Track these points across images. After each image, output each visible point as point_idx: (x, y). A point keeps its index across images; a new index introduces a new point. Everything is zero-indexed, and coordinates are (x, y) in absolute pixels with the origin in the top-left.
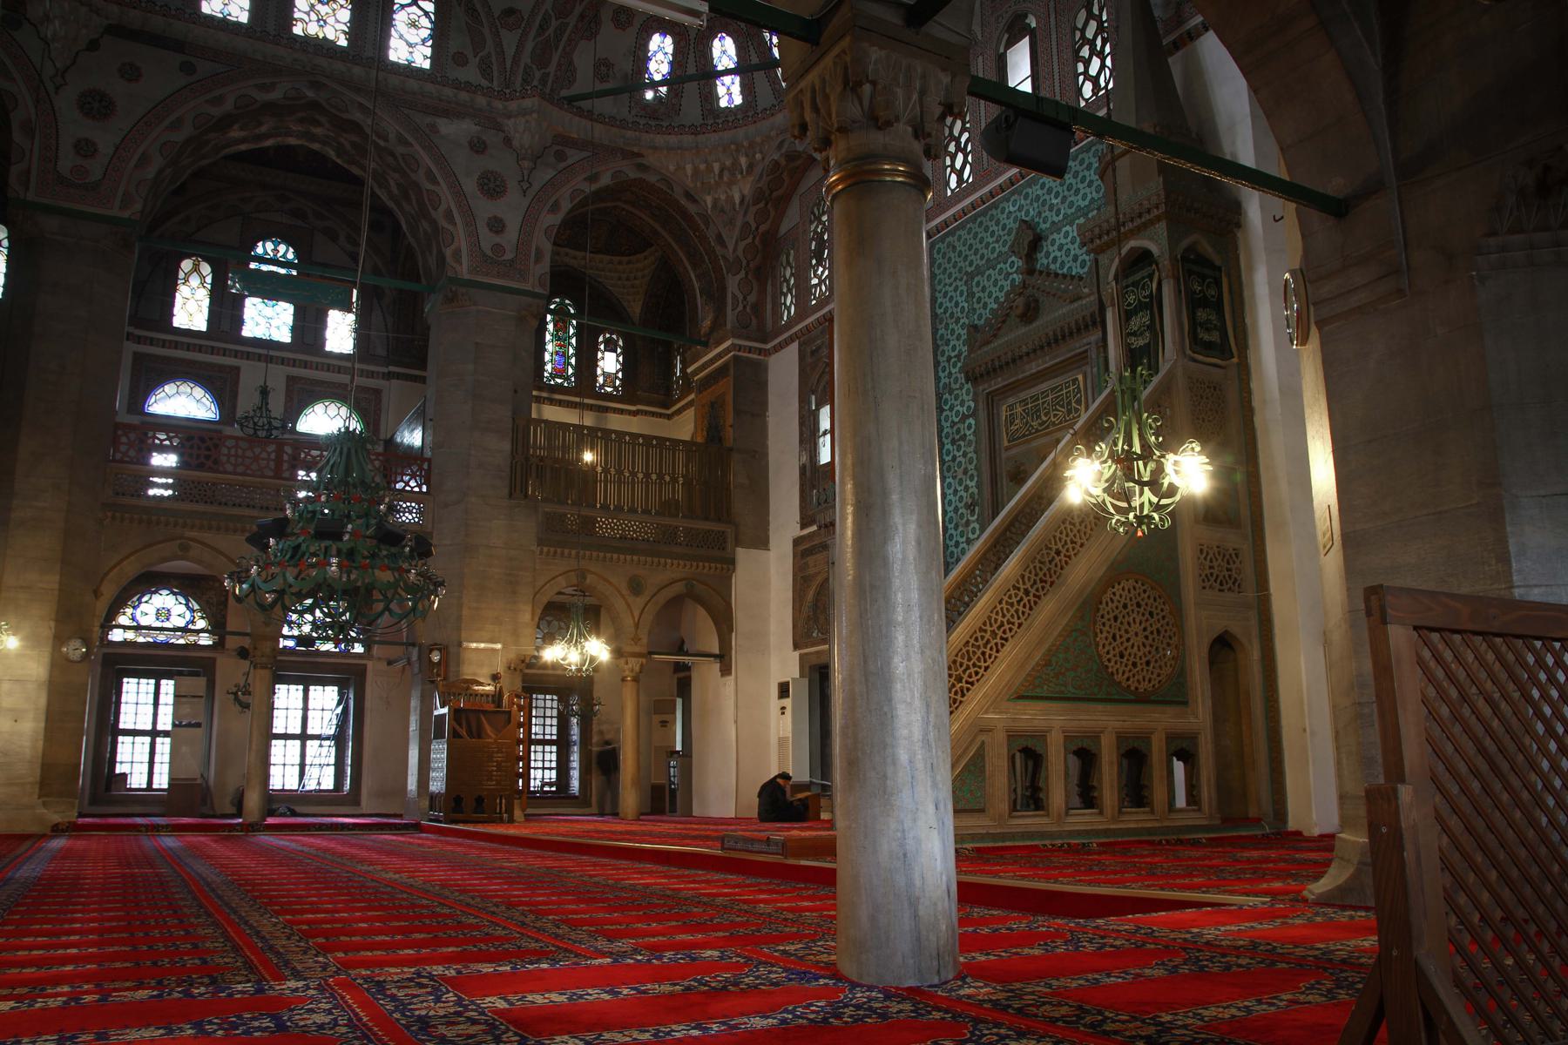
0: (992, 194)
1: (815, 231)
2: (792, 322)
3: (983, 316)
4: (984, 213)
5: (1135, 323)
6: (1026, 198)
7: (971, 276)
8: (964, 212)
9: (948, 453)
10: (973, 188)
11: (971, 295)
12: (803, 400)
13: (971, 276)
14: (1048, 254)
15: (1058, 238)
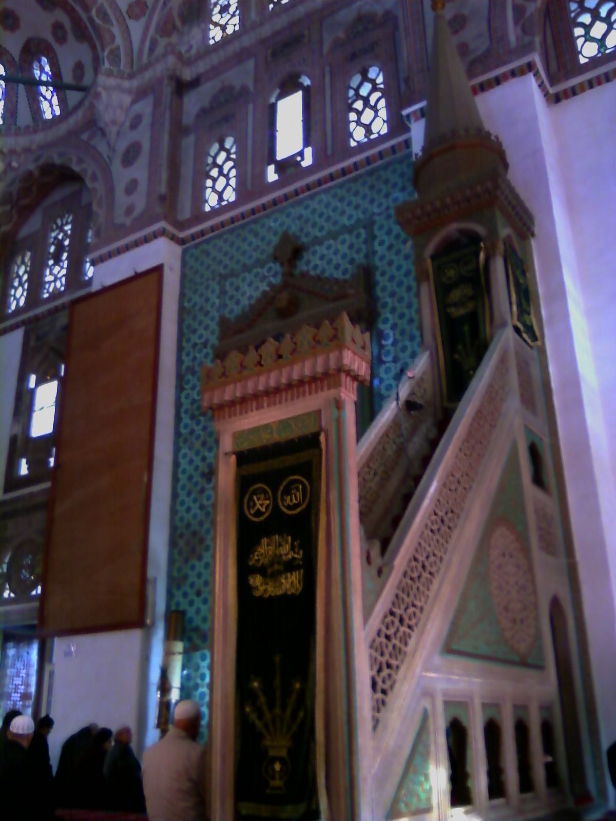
0: (253, 212)
1: (56, 238)
2: (19, 311)
3: (234, 310)
4: (243, 227)
5: (455, 295)
6: (288, 215)
7: (224, 277)
8: (223, 224)
9: (186, 426)
10: (231, 206)
11: (223, 292)
12: (22, 379)
13: (224, 277)
14: (308, 262)
15: (321, 250)
